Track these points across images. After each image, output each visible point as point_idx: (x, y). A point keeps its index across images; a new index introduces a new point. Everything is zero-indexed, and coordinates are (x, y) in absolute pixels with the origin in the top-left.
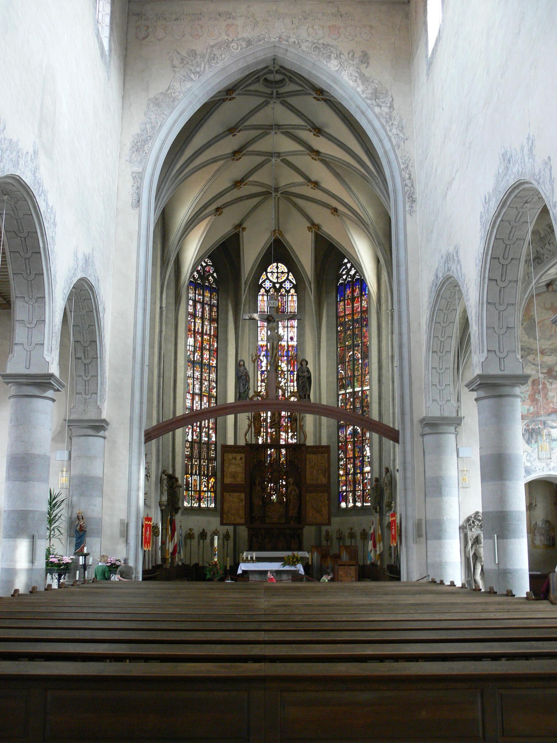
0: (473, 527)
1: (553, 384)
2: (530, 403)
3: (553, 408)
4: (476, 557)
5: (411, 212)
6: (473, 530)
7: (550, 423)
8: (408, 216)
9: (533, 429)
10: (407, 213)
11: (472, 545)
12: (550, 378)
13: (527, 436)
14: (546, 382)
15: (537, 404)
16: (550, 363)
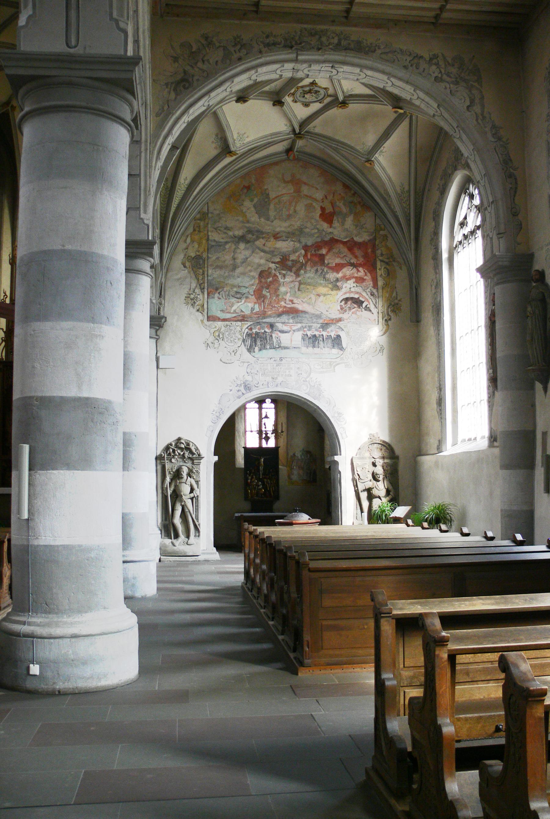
0: (173, 457)
1: (287, 277)
2: (256, 301)
3: (285, 307)
4: (177, 495)
6: (173, 460)
7: (280, 326)
9: (257, 334)
11: (172, 480)
12: (283, 270)
13: (249, 342)
14: (278, 274)
15: (263, 301)
16: (284, 250)
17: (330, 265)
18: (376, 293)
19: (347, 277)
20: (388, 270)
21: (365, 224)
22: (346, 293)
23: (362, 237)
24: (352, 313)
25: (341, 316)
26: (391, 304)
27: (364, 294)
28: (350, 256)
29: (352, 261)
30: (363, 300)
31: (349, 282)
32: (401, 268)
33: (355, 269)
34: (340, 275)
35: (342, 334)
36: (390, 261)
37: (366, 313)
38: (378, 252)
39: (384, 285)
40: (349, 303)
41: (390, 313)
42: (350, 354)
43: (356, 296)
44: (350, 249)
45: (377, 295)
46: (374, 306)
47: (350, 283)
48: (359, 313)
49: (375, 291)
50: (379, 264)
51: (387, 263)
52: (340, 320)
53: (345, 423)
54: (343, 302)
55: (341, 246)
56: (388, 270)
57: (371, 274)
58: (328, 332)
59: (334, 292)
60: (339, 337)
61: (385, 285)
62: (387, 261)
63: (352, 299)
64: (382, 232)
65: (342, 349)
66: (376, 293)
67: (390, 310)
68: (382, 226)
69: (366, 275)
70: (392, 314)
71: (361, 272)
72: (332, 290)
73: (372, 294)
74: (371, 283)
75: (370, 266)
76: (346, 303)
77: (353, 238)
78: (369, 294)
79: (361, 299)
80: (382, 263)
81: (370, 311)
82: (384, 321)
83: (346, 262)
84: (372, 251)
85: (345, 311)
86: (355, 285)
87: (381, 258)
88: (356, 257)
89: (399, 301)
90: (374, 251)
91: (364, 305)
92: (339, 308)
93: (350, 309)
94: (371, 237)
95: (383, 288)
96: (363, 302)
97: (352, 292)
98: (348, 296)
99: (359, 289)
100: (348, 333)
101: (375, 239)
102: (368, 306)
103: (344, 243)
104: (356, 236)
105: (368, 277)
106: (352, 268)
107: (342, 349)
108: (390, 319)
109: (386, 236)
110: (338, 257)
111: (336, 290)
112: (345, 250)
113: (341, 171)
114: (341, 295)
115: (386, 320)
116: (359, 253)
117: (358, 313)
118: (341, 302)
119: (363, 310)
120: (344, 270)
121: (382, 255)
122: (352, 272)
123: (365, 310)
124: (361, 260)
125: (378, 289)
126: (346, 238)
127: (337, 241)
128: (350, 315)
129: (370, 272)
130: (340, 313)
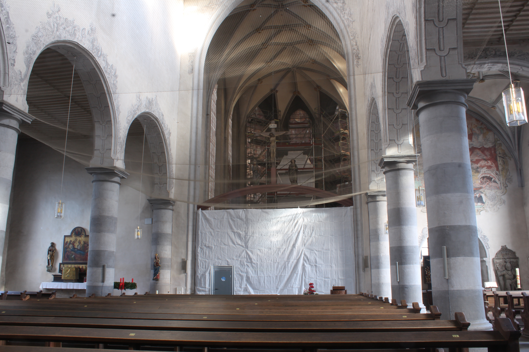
5: (358, 65)
8: (356, 68)
10: (355, 66)
17: (473, 160)
18: (498, 173)
19: (483, 166)
20: (503, 161)
21: (489, 138)
22: (482, 174)
23: (489, 145)
24: (487, 184)
25: (481, 186)
26: (507, 179)
27: (492, 174)
28: (483, 155)
29: (484, 158)
30: (492, 177)
31: (483, 168)
32: (510, 160)
33: (486, 161)
34: (479, 165)
35: (483, 195)
36: (504, 156)
37: (493, 184)
38: (498, 152)
39: (502, 169)
40: (485, 179)
41: (507, 183)
42: (488, 205)
43: (488, 175)
44: (483, 152)
45: (499, 174)
46: (498, 180)
47: (484, 170)
48: (490, 184)
49: (498, 172)
50: (498, 159)
51: (503, 158)
52: (481, 188)
53: (488, 241)
54: (482, 179)
55: (478, 150)
56: (503, 161)
57: (495, 164)
58: (475, 194)
59: (476, 174)
60: (481, 197)
61: (503, 169)
62: (503, 156)
63: (486, 177)
64: (498, 142)
65: (483, 203)
66: (498, 173)
67: (506, 181)
68: (498, 139)
69: (492, 164)
70: (508, 184)
71: (490, 163)
72: (475, 173)
73: (497, 174)
74: (495, 168)
75: (494, 159)
76: (483, 179)
77: (483, 146)
78: (495, 174)
79: (491, 177)
80: (500, 158)
81: (496, 182)
82: (504, 187)
83: (481, 158)
84: (494, 152)
85: (483, 183)
86: (487, 170)
87: (499, 155)
88: (486, 155)
89: (511, 176)
90: (495, 152)
91: (493, 180)
92: (480, 182)
93: (486, 182)
94: (493, 145)
95: (502, 171)
96: (492, 178)
97: (486, 174)
98: (484, 175)
99: (489, 172)
100: (485, 195)
101: (495, 146)
102: (495, 180)
103: (479, 149)
104: (485, 145)
105: (494, 165)
106: (484, 161)
107: (483, 203)
108: (507, 186)
109: (501, 144)
110: (477, 156)
111: (478, 173)
112: (480, 152)
113: (474, 113)
114: (480, 175)
115: (505, 187)
116: (487, 153)
117: (490, 184)
118: (481, 179)
119: (492, 182)
120: (481, 162)
121: (500, 154)
122: (485, 163)
123: (494, 182)
124: (489, 157)
125: (499, 171)
126: (479, 147)
127: (476, 148)
128: (486, 185)
129: (494, 163)
130: (481, 185)
